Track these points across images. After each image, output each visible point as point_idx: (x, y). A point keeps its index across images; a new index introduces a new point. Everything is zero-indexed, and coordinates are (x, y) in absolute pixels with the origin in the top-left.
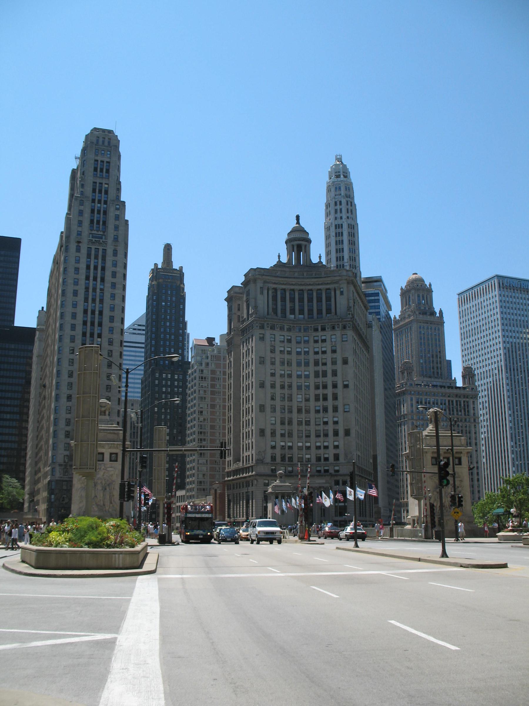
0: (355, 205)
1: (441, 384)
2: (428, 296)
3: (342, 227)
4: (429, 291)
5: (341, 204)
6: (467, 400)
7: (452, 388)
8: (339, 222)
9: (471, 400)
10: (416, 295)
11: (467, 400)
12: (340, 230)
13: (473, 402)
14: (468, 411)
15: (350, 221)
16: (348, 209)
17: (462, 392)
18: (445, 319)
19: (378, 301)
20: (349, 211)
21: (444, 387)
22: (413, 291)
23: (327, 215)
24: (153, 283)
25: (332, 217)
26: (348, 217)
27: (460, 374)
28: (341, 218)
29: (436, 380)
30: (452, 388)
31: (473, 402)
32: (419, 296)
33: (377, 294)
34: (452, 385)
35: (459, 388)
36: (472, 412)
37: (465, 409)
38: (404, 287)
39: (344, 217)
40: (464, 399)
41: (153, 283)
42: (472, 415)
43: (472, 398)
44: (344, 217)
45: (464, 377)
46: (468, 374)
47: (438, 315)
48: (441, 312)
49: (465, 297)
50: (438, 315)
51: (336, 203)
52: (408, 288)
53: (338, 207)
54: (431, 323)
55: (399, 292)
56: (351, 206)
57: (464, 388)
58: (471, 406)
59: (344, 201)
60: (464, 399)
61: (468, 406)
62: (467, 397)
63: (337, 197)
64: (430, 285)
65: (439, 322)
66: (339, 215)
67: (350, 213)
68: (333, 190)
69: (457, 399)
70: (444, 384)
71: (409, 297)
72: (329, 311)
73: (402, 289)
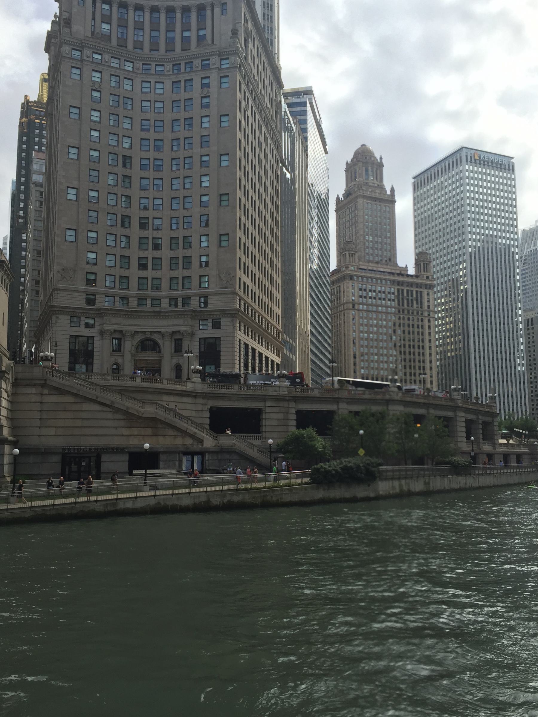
1: (389, 271)
2: (378, 172)
4: (380, 165)
6: (421, 290)
7: (402, 275)
9: (425, 292)
10: (364, 168)
11: (421, 290)
13: (428, 294)
14: (421, 303)
17: (415, 280)
18: (397, 198)
19: (305, 113)
21: (393, 274)
22: (360, 164)
24: (23, 120)
27: (413, 262)
29: (385, 266)
30: (402, 275)
31: (428, 294)
32: (367, 170)
33: (305, 104)
34: (402, 272)
35: (411, 276)
36: (426, 304)
37: (417, 300)
38: (349, 161)
40: (417, 289)
41: (23, 120)
42: (426, 308)
43: (426, 288)
45: (417, 264)
46: (422, 260)
47: (389, 193)
48: (393, 190)
49: (421, 181)
50: (389, 193)
52: (355, 160)
54: (381, 200)
55: (344, 167)
57: (417, 276)
60: (417, 289)
61: (421, 296)
62: (421, 287)
64: (381, 158)
65: (390, 201)
69: (408, 288)
70: (393, 271)
71: (355, 173)
72: (200, 39)
73: (347, 163)
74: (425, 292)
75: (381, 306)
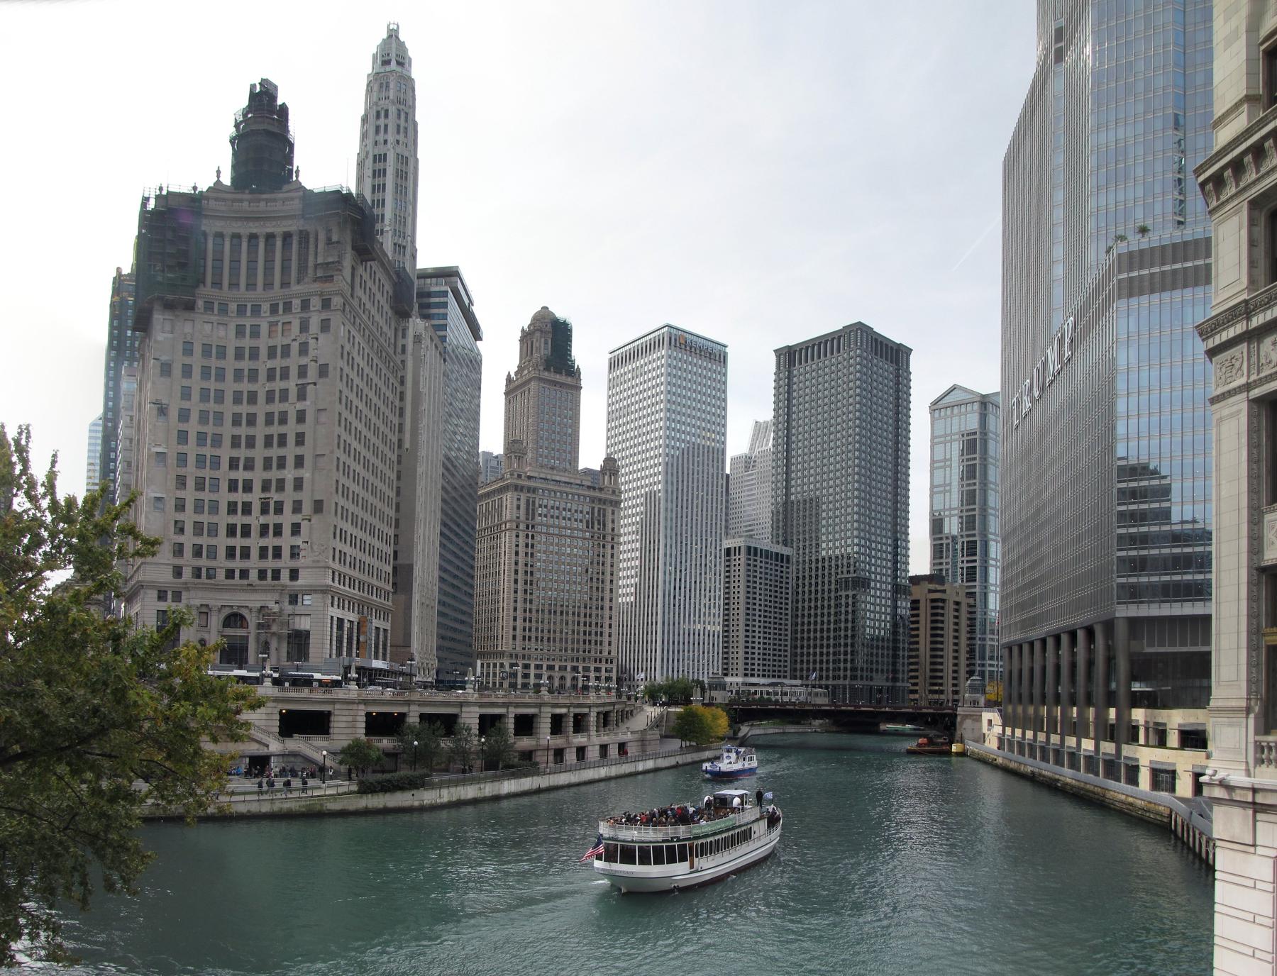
0: (415, 124)
3: (385, 160)
5: (386, 116)
8: (381, 150)
12: (380, 166)
15: (400, 150)
16: (398, 126)
20: (402, 130)
23: (364, 136)
25: (370, 141)
26: (398, 142)
28: (386, 142)
36: (610, 526)
39: (391, 139)
44: (391, 139)
51: (378, 114)
53: (382, 122)
56: (406, 121)
58: (609, 517)
59: (393, 110)
63: (381, 102)
66: (381, 138)
67: (402, 135)
68: (376, 88)
74: (609, 510)
75: (553, 526)
